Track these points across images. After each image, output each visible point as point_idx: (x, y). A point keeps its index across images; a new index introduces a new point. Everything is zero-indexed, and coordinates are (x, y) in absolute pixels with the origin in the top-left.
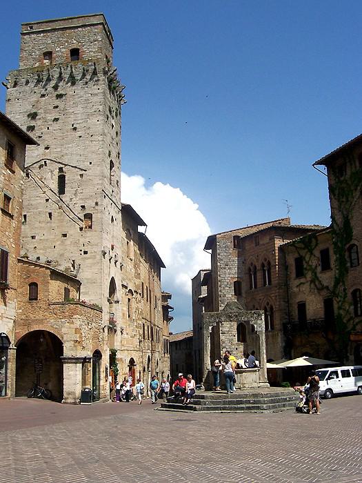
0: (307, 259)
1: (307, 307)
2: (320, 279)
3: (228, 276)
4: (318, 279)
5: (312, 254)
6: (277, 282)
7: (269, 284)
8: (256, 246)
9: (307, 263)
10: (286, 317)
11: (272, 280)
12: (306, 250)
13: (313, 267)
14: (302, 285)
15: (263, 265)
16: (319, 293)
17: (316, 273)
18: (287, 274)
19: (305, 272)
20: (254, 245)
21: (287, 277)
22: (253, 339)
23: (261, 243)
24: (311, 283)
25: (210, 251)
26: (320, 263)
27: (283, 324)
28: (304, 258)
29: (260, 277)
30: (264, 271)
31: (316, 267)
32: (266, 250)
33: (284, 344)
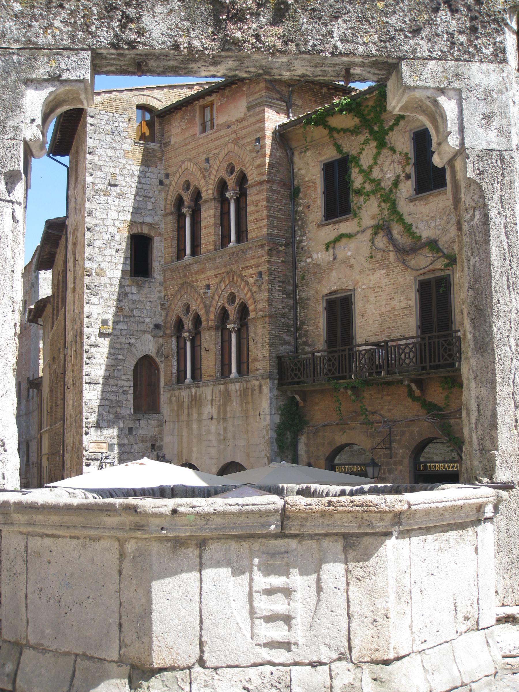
0: (366, 161)
1: (359, 306)
2: (408, 220)
3: (113, 215)
4: (400, 219)
5: (382, 144)
6: (265, 231)
7: (239, 240)
8: (204, 131)
9: (366, 174)
10: (288, 338)
11: (251, 227)
12: (361, 138)
13: (387, 184)
14: (344, 241)
15: (222, 186)
16: (403, 262)
17: (394, 205)
18: (295, 212)
19: (356, 201)
20: (197, 129)
21: (295, 221)
22: (180, 406)
23: (221, 119)
24: (376, 233)
25: (66, 160)
26: (410, 169)
27: (279, 358)
28: (356, 160)
29: (212, 221)
30: (224, 202)
31: (396, 183)
32: (235, 142)
33: (277, 419)
